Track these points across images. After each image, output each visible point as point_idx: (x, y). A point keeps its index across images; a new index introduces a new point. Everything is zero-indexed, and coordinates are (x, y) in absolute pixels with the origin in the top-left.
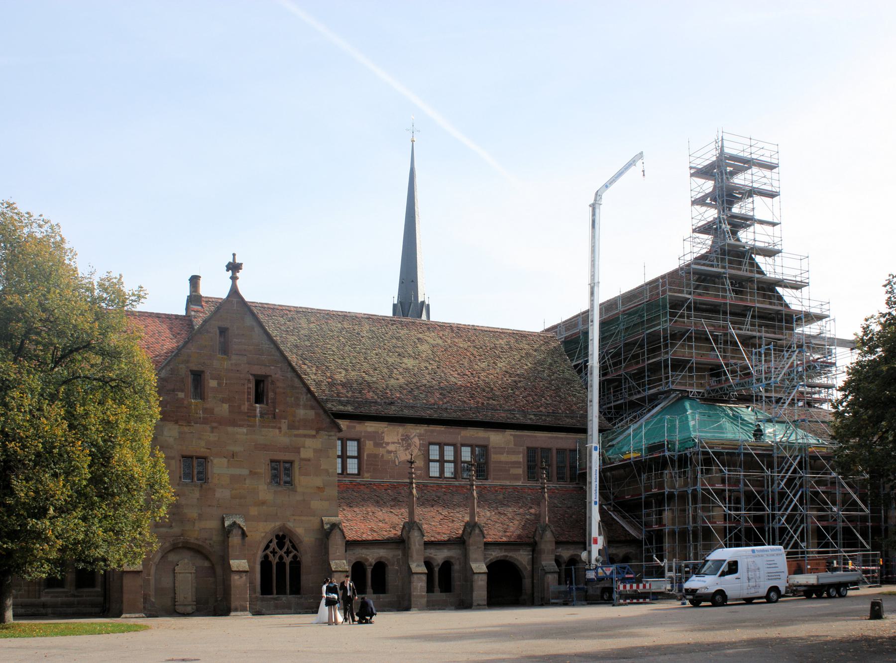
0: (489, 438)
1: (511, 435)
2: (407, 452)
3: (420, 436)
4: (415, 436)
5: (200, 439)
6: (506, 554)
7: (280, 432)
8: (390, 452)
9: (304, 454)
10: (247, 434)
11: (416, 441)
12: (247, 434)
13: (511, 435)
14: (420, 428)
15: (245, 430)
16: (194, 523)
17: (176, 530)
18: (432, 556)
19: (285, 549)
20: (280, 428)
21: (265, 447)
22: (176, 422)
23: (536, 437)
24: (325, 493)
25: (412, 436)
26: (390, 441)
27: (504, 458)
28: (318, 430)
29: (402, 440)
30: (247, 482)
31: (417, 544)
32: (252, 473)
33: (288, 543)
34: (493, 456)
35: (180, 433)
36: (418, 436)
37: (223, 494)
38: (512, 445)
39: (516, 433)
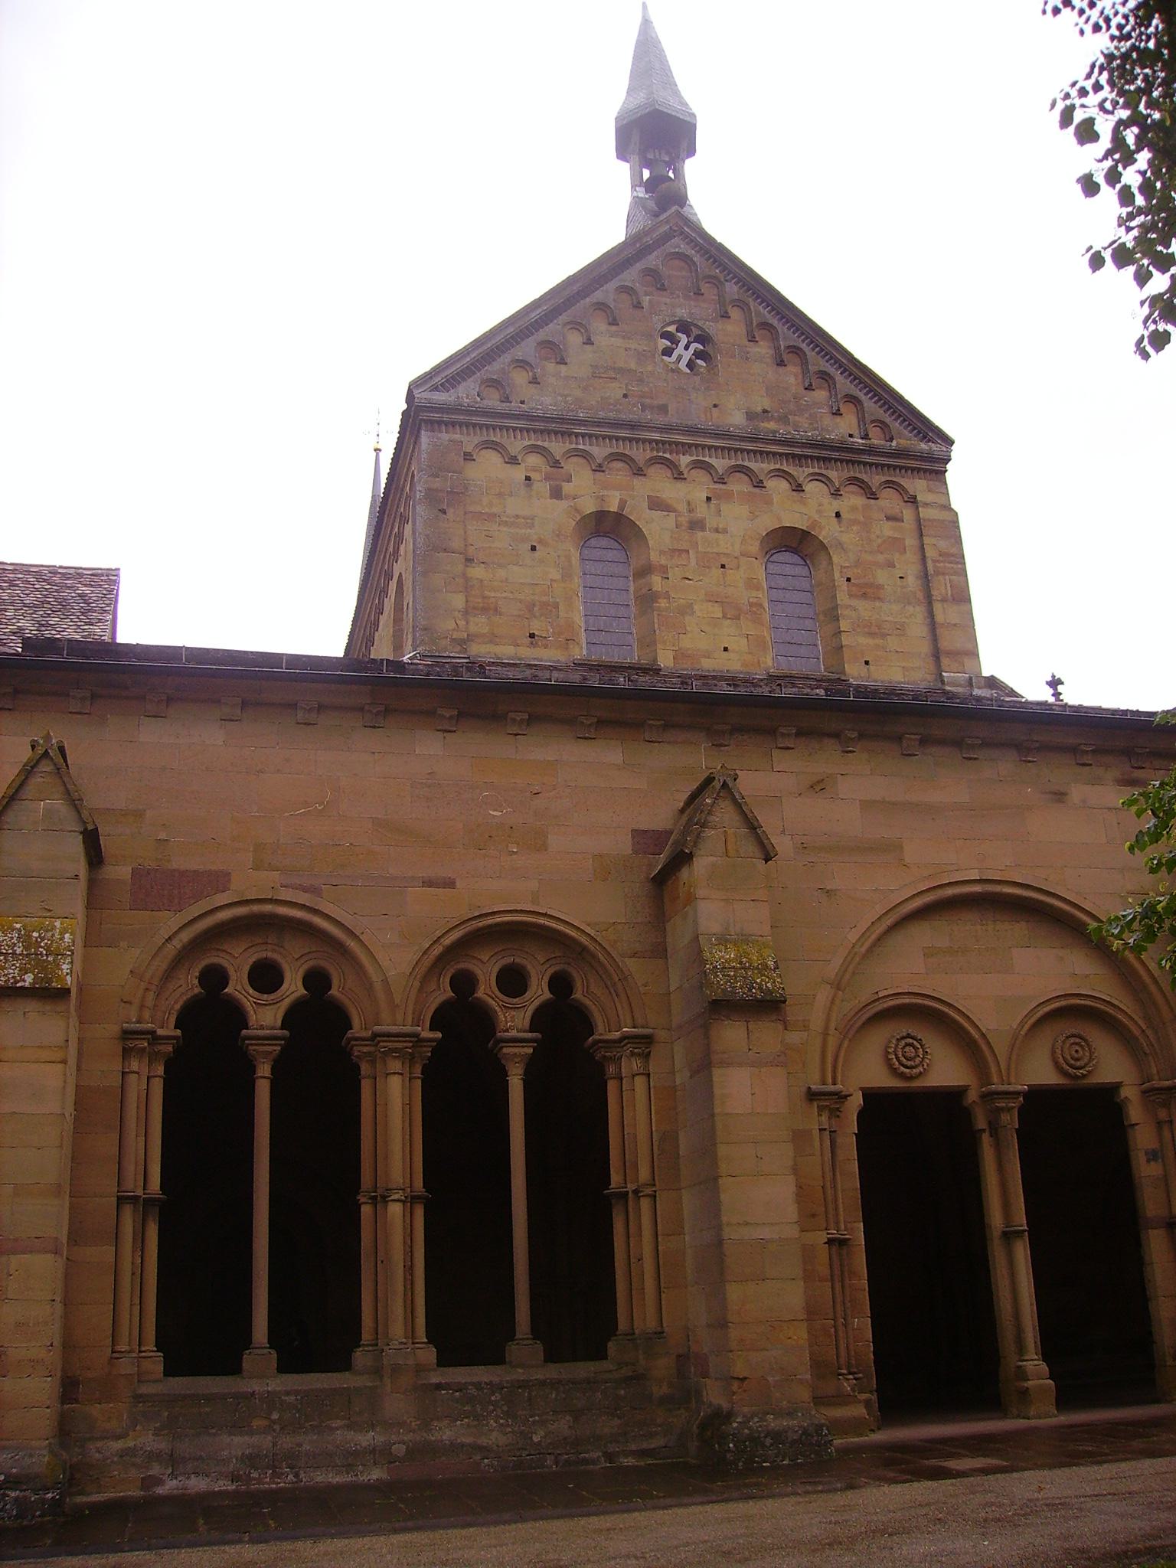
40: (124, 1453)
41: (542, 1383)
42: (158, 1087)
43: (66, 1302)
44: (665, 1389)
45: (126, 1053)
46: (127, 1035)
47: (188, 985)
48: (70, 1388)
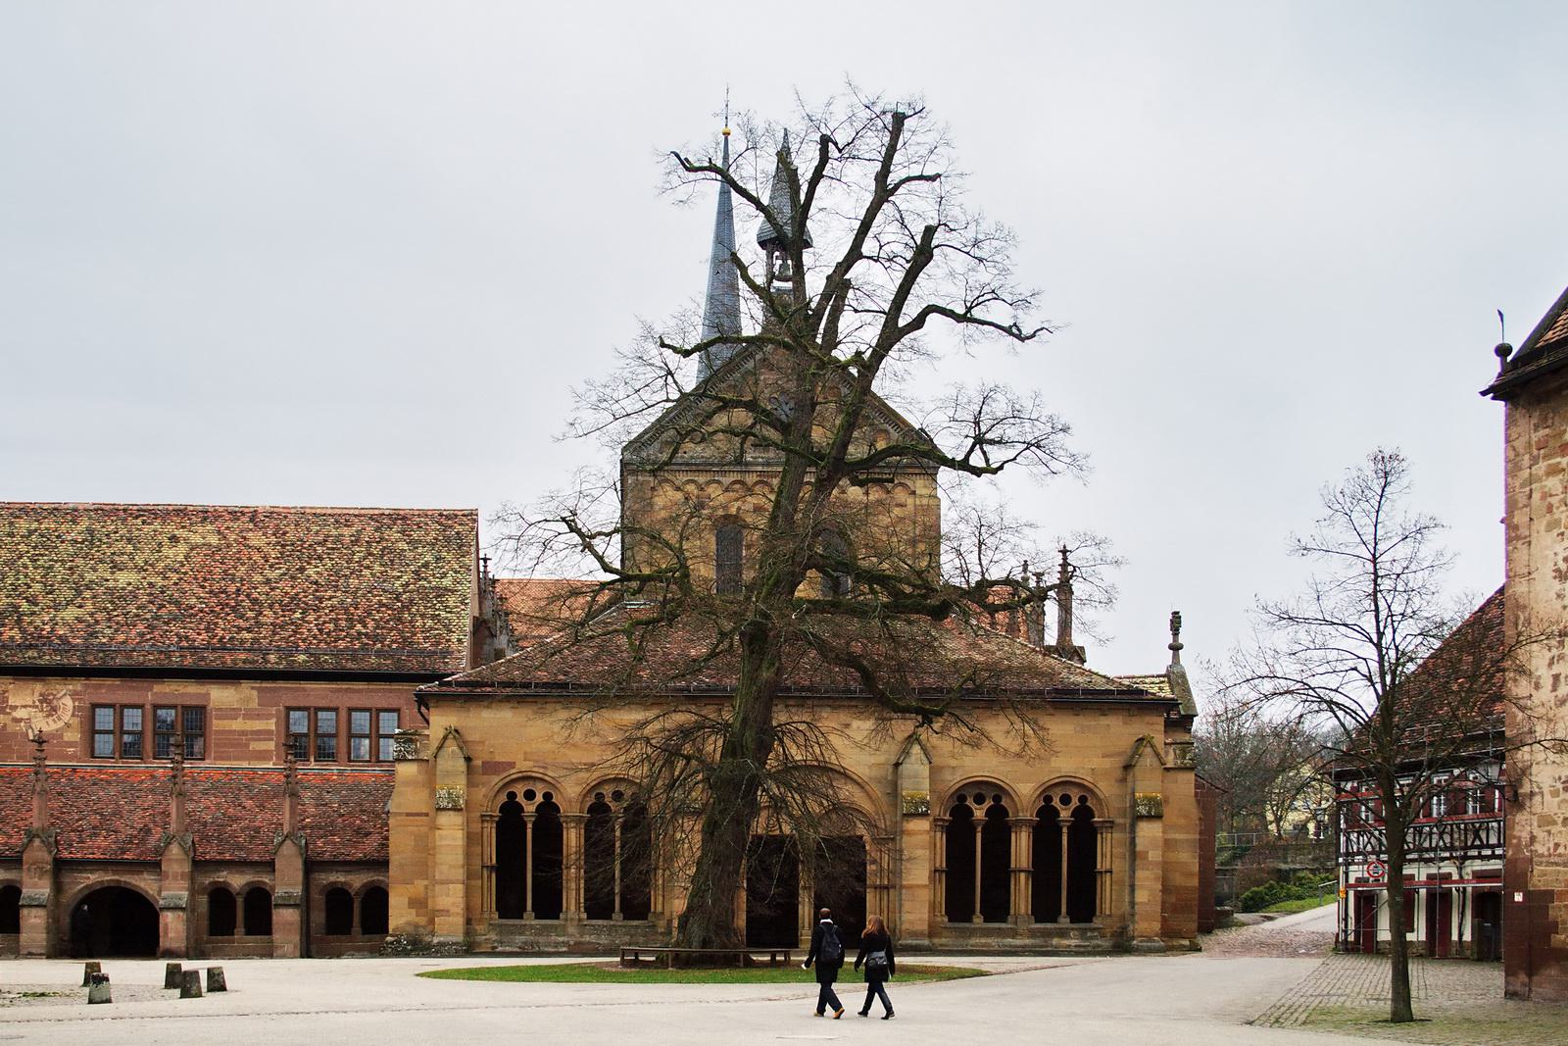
1: (253, 688)
2: (50, 720)
3: (74, 695)
4: (65, 694)
6: (116, 877)
8: (17, 721)
11: (68, 702)
14: (76, 682)
23: (304, 690)
25: (59, 696)
27: (237, 725)
29: (41, 702)
34: (214, 722)
38: (254, 704)
39: (264, 685)
40: (486, 939)
41: (620, 926)
42: (494, 831)
43: (467, 897)
44: (663, 930)
45: (483, 821)
46: (482, 816)
47: (503, 798)
48: (468, 921)
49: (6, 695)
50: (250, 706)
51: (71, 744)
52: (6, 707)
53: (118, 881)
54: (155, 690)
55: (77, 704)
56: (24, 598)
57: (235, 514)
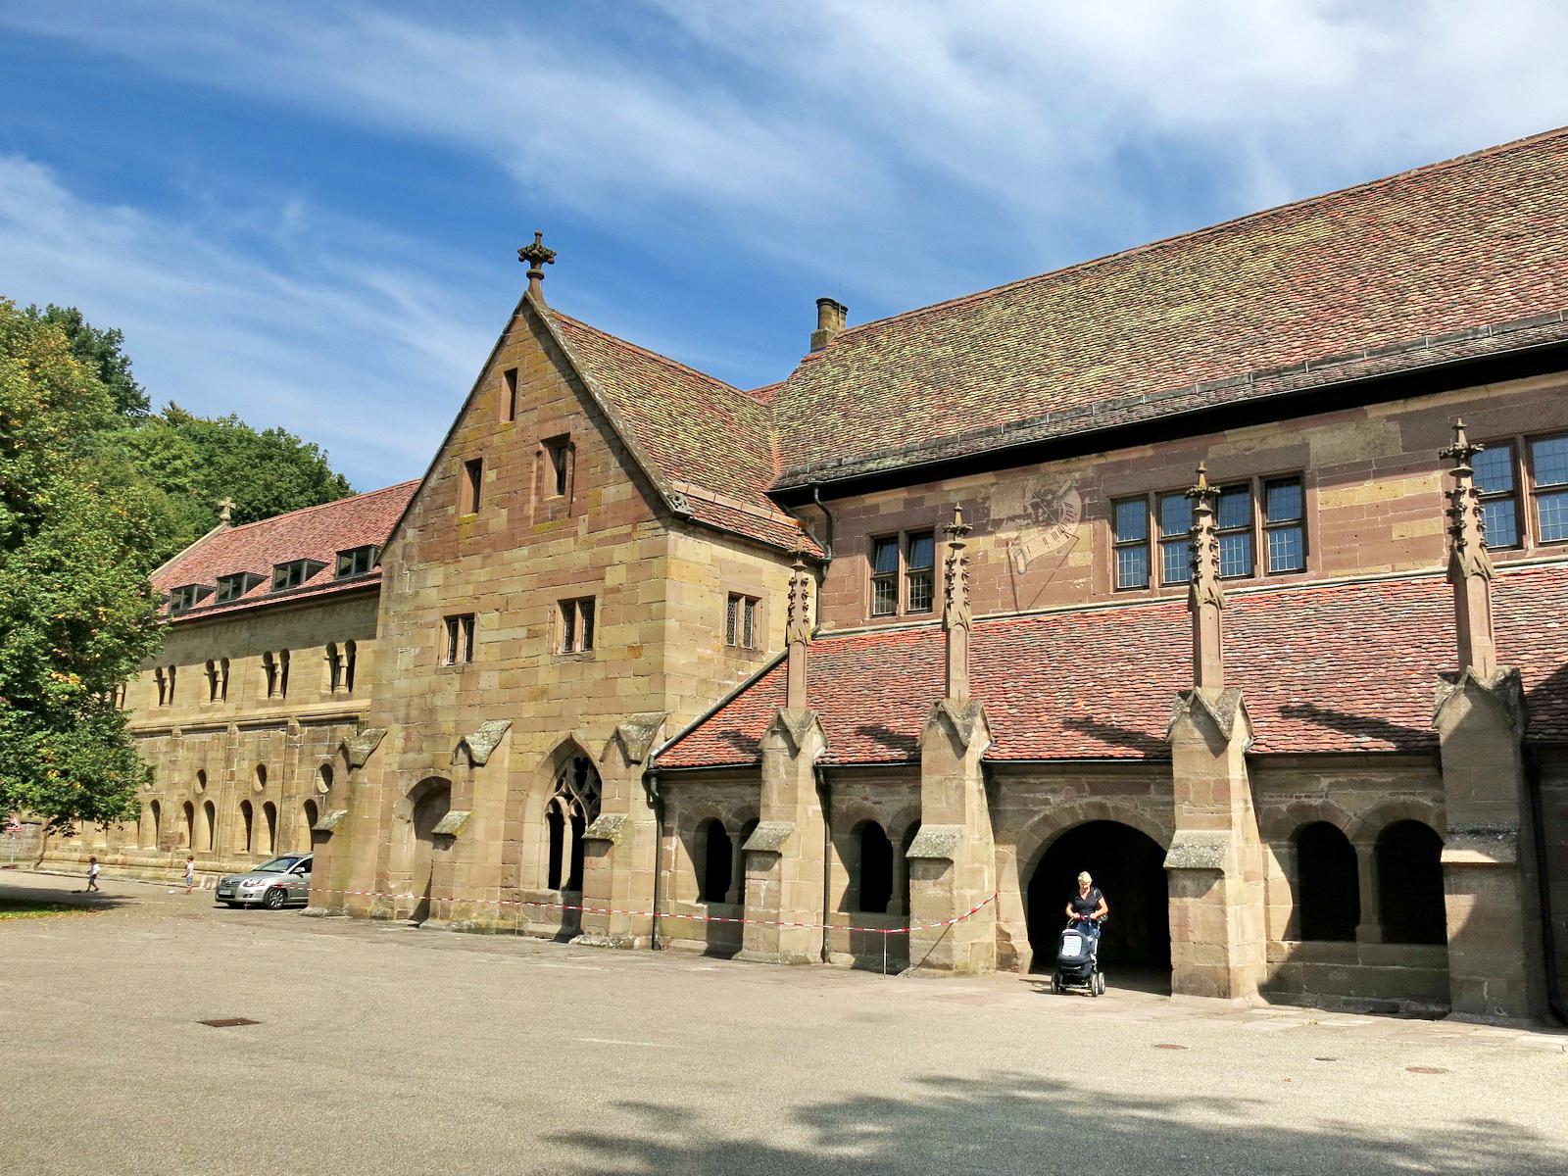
0: (1306, 446)
1: (1389, 418)
3: (1083, 487)
4: (1070, 489)
5: (467, 583)
6: (1098, 799)
7: (576, 541)
9: (614, 577)
10: (529, 558)
12: (529, 558)
13: (1389, 418)
15: (525, 551)
16: (449, 741)
17: (426, 757)
18: (868, 804)
19: (586, 790)
20: (576, 533)
21: (550, 579)
22: (442, 560)
24: (643, 658)
25: (1060, 493)
26: (1002, 516)
28: (637, 520)
29: (1031, 505)
30: (524, 653)
31: (782, 769)
32: (533, 635)
33: (589, 773)
35: (447, 577)
36: (1076, 488)
37: (489, 680)
49: (987, 505)
50: (1388, 453)
51: (1079, 572)
52: (987, 524)
53: (1102, 807)
54: (1210, 456)
55: (1087, 501)
56: (1036, 372)
57: (1357, 195)
